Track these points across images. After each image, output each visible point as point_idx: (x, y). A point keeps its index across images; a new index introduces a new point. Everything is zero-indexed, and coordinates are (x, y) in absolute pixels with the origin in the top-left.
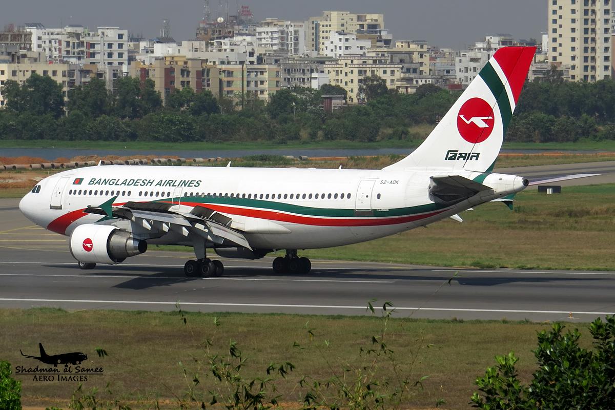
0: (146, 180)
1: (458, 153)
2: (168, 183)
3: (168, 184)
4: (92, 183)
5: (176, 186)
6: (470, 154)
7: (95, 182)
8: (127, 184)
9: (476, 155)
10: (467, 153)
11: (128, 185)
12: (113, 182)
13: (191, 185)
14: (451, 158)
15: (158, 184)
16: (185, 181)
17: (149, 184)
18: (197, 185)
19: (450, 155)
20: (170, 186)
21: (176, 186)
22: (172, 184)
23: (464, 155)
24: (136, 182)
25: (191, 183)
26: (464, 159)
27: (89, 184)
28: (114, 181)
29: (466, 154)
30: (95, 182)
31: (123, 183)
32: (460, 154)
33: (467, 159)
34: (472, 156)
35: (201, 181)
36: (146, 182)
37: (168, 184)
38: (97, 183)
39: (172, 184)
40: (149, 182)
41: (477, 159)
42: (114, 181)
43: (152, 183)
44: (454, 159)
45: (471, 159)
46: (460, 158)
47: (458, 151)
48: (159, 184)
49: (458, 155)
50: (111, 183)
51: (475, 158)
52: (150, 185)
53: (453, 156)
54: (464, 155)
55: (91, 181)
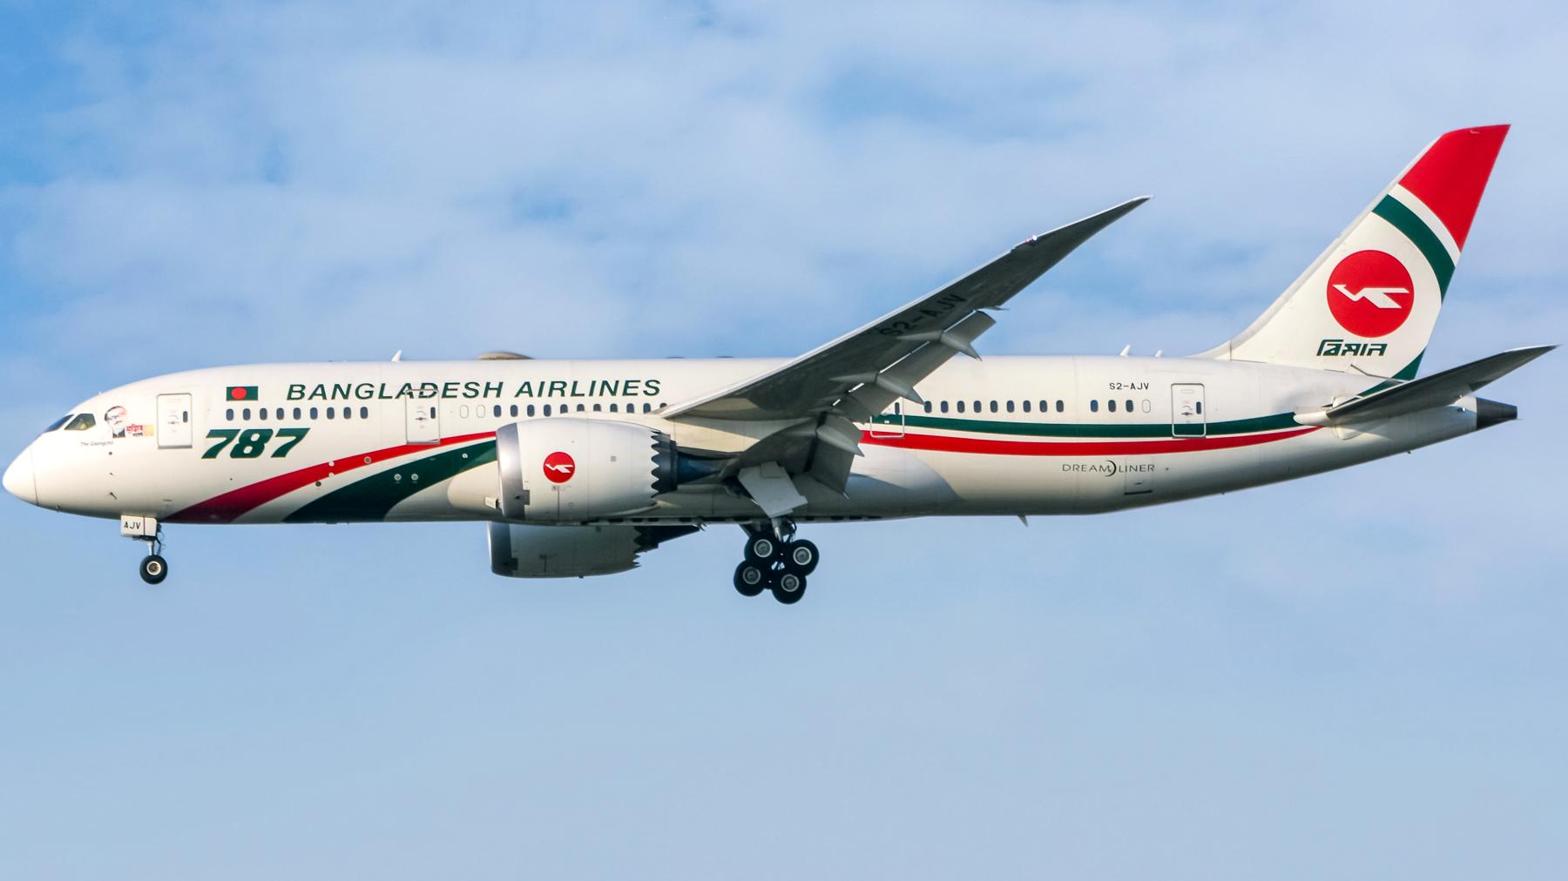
0: (477, 384)
1: (1343, 344)
2: (552, 388)
3: (556, 393)
4: (294, 395)
5: (583, 395)
6: (1365, 346)
7: (308, 393)
8: (416, 394)
9: (1380, 347)
10: (1360, 345)
11: (421, 395)
12: (371, 392)
13: (629, 391)
14: (1328, 353)
15: (521, 391)
16: (605, 383)
17: (492, 393)
18: (652, 391)
19: (1326, 348)
20: (563, 394)
21: (583, 395)
22: (568, 390)
23: (1354, 348)
24: (446, 389)
25: (627, 386)
26: (1355, 354)
27: (289, 398)
29: (1358, 346)
30: (308, 393)
31: (401, 393)
32: (1346, 345)
33: (1362, 354)
34: (1371, 351)
35: (658, 382)
36: (481, 390)
37: (556, 393)
38: (314, 394)
39: (568, 390)
40: (488, 387)
41: (1381, 354)
42: (370, 389)
43: (499, 390)
44: (1336, 354)
45: (1369, 354)
46: (1347, 353)
47: (1342, 341)
48: (526, 388)
49: (1343, 348)
50: (361, 393)
51: (1379, 352)
52: (498, 395)
53: (1331, 349)
54: (1354, 348)
55: (291, 391)
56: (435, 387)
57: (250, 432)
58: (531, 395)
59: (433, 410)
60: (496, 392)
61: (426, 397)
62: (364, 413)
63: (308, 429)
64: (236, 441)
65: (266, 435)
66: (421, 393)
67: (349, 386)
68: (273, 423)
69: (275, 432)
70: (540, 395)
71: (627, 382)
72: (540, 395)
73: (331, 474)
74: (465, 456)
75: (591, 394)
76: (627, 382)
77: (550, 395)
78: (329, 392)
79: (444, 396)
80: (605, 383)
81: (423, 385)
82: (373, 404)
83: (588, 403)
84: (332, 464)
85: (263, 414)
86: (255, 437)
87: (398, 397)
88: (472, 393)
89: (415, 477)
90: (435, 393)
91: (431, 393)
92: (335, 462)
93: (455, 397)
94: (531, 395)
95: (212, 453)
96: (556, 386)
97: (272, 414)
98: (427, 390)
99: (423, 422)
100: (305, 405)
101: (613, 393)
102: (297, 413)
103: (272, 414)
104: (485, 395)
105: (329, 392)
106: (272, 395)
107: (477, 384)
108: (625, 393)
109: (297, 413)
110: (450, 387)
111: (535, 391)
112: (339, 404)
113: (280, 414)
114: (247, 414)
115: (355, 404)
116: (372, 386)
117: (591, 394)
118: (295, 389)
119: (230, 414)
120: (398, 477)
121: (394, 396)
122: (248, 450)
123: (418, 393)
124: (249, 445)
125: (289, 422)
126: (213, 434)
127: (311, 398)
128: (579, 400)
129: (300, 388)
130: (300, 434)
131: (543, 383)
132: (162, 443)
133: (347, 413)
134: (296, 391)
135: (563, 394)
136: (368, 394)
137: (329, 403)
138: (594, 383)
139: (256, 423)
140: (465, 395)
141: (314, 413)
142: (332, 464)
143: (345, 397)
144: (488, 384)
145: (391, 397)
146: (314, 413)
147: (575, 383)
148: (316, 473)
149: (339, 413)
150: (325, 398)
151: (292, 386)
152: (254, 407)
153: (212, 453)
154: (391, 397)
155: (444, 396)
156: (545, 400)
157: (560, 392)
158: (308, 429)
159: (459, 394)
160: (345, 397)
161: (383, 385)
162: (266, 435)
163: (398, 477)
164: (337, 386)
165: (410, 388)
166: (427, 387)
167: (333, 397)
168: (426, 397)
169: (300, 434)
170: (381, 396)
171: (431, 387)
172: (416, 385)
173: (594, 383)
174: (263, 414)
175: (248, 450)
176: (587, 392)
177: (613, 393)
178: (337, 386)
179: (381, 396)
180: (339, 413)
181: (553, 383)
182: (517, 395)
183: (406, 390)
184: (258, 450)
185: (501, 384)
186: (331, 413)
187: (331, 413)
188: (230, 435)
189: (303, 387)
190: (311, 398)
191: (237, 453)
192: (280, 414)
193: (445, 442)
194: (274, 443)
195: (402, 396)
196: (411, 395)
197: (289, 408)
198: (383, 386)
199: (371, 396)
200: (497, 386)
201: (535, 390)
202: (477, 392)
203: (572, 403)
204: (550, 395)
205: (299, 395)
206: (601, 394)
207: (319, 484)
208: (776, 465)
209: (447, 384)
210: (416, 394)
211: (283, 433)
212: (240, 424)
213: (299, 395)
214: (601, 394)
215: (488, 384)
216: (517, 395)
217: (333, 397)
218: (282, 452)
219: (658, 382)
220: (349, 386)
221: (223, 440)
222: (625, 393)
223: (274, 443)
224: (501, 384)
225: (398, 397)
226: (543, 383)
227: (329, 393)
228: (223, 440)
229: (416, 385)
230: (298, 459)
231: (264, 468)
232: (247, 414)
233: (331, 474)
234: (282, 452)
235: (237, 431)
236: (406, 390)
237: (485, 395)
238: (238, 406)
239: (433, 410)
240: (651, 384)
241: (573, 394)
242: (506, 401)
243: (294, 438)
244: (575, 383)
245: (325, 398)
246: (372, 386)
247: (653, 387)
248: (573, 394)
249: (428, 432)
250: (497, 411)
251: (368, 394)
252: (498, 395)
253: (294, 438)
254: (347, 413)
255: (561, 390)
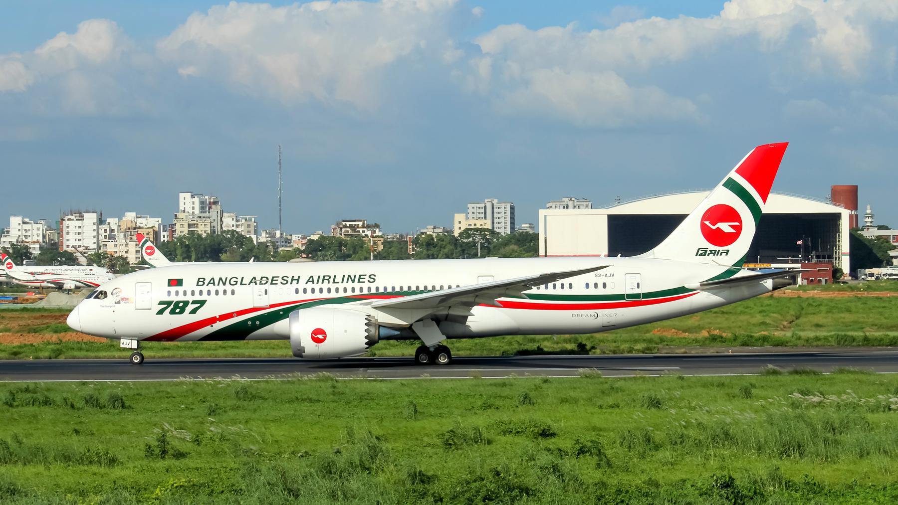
0: (288, 277)
2: (324, 279)
4: (200, 283)
5: (338, 283)
7: (206, 282)
8: (258, 282)
11: (261, 283)
12: (237, 282)
13: (361, 280)
15: (308, 281)
16: (349, 276)
18: (372, 280)
20: (329, 283)
21: (338, 283)
22: (331, 280)
24: (273, 280)
25: (360, 278)
28: (235, 280)
30: (206, 282)
31: (251, 282)
35: (375, 276)
38: (209, 283)
39: (331, 280)
40: (293, 279)
42: (235, 280)
43: (298, 280)
48: (311, 280)
50: (232, 282)
52: (297, 283)
55: (199, 281)
56: (267, 279)
57: (178, 302)
58: (313, 283)
59: (266, 291)
60: (296, 281)
61: (263, 284)
62: (233, 293)
63: (206, 301)
64: (172, 306)
65: (186, 303)
66: (261, 282)
67: (226, 278)
68: (189, 298)
69: (190, 302)
70: (318, 283)
71: (360, 276)
72: (318, 283)
73: (218, 322)
74: (281, 313)
75: (342, 282)
76: (360, 276)
77: (323, 283)
78: (216, 282)
79: (272, 284)
80: (349, 276)
81: (262, 278)
82: (237, 287)
83: (341, 287)
84: (218, 317)
85: (185, 293)
86: (181, 305)
87: (249, 284)
88: (285, 282)
89: (258, 323)
90: (267, 282)
91: (265, 282)
92: (219, 316)
93: (277, 284)
94: (313, 283)
95: (161, 312)
96: (328, 278)
97: (189, 293)
98: (264, 280)
99: (261, 297)
100: (205, 289)
101: (353, 281)
102: (201, 293)
103: (189, 293)
104: (291, 283)
105: (216, 283)
106: (189, 284)
107: (288, 277)
108: (359, 282)
109: (201, 293)
110: (274, 279)
111: (315, 281)
112: (221, 288)
113: (193, 293)
114: (177, 293)
115: (228, 288)
116: (237, 279)
117: (342, 282)
118: (201, 280)
119: (169, 292)
120: (249, 323)
121: (248, 283)
122: (178, 310)
123: (259, 282)
124: (178, 308)
125: (197, 297)
126: (161, 303)
127: (207, 285)
128: (336, 285)
129: (202, 280)
130: (202, 303)
131: (319, 277)
132: (137, 307)
133: (225, 292)
134: (200, 281)
135: (329, 283)
136: (235, 283)
137: (216, 287)
138: (344, 276)
139: (181, 298)
140: (281, 283)
141: (209, 293)
142: (218, 317)
143: (224, 284)
144: (293, 277)
145: (246, 284)
146: (209, 293)
147: (335, 276)
148: (211, 321)
149: (221, 292)
150: (214, 285)
151: (199, 279)
152: (180, 289)
153: (161, 312)
154: (246, 284)
155: (272, 284)
156: (320, 285)
157: (327, 281)
158: (206, 301)
159: (278, 282)
160: (224, 284)
161: (243, 278)
162: (186, 303)
163: (249, 323)
164: (221, 279)
165: (255, 279)
166: (263, 279)
167: (218, 285)
168: (263, 284)
169: (202, 303)
170: (241, 284)
171: (265, 279)
172: (258, 278)
173: (344, 276)
174: (185, 293)
175: (178, 310)
176: (340, 281)
177: (353, 281)
178: (221, 279)
179: (241, 284)
180: (221, 292)
181: (324, 276)
182: (307, 283)
183: (253, 280)
184: (182, 312)
185: (299, 277)
186: (217, 293)
187: (217, 293)
188: (169, 303)
189: (204, 279)
190: (207, 285)
191: (173, 312)
192: (193, 293)
193: (272, 306)
194: (190, 307)
195: (251, 284)
196: (256, 283)
197: (197, 290)
198: (243, 278)
199: (236, 284)
200: (297, 278)
201: (315, 281)
202: (287, 281)
203: (333, 287)
204: (323, 283)
205: (202, 283)
206: (347, 282)
207: (212, 326)
208: (431, 320)
209: (273, 277)
210: (258, 282)
211: (194, 302)
212: (174, 298)
213: (202, 283)
214: (347, 282)
215: (293, 277)
216: (307, 283)
217: (218, 285)
218: (194, 312)
219: (375, 276)
220: (226, 278)
221: (166, 306)
222: (359, 282)
223: (190, 307)
224: (299, 277)
225: (249, 284)
226: (319, 277)
227: (216, 283)
228: (166, 306)
229: (258, 278)
230: (201, 315)
231: (185, 319)
232: (177, 293)
233: (218, 322)
234: (194, 312)
235: (173, 301)
236: (253, 280)
237: (291, 283)
238: (173, 289)
239: (266, 291)
240: (372, 276)
241: (334, 282)
242: (302, 285)
243: (199, 305)
244: (335, 276)
245: (214, 285)
246: (237, 279)
247: (372, 278)
248: (334, 282)
249: (263, 301)
250: (297, 291)
251: (235, 283)
252: (297, 283)
253: (199, 305)
254: (225, 292)
255: (328, 280)
